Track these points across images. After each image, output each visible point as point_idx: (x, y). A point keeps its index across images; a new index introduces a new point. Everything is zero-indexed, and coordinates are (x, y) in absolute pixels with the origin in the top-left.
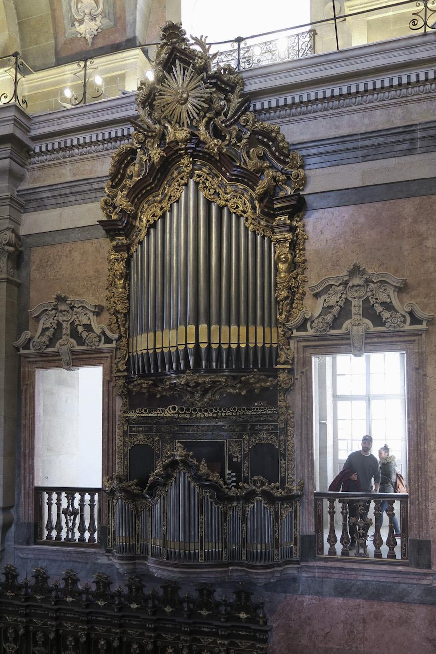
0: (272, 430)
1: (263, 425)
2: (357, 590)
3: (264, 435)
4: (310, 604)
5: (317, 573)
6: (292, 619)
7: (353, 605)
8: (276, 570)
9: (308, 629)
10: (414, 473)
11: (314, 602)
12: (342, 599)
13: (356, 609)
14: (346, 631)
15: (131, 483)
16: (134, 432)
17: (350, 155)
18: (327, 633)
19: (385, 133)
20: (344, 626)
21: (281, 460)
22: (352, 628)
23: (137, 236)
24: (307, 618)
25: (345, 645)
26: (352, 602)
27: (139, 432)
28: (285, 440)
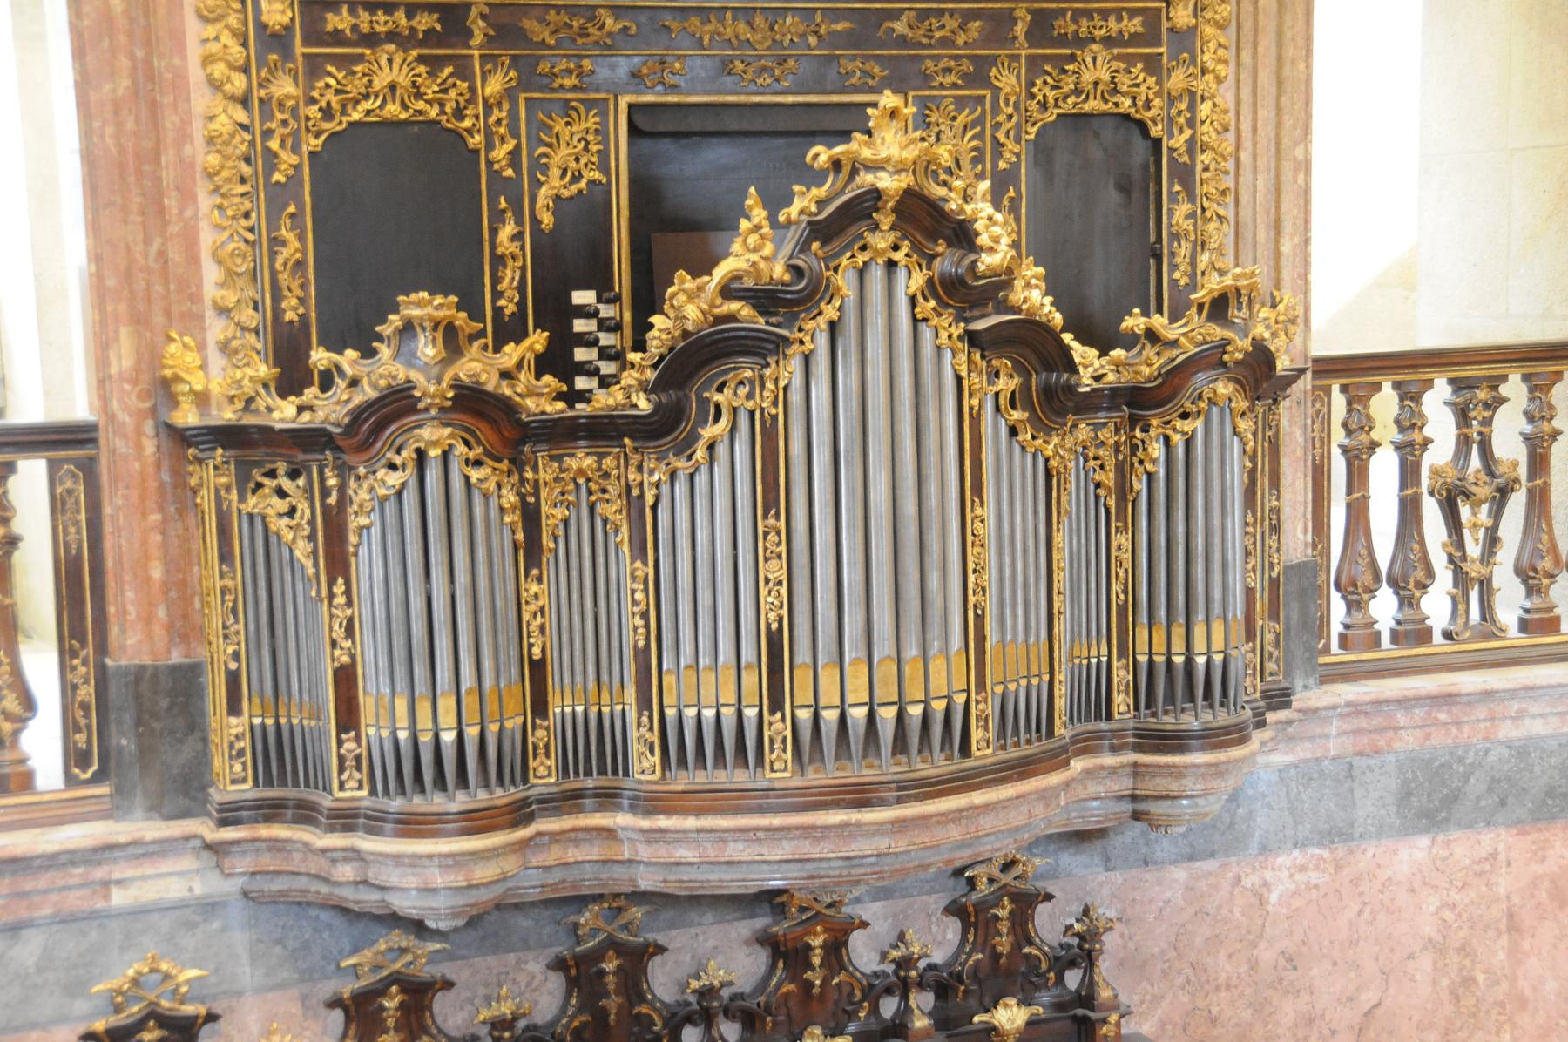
0: (1135, 40)
1: (1089, 14)
2: (1490, 789)
3: (1096, 67)
4: (1295, 894)
5: (1335, 741)
6: (1223, 978)
7: (1467, 862)
8: (540, 834)
9: (1288, 1011)
11: (1314, 877)
12: (1424, 841)
13: (1480, 874)
14: (1445, 982)
15: (511, 353)
16: (337, 38)
18: (1368, 1013)
20: (1435, 963)
21: (1173, 198)
22: (1467, 962)
24: (1282, 962)
27: (371, 40)
28: (1192, 94)
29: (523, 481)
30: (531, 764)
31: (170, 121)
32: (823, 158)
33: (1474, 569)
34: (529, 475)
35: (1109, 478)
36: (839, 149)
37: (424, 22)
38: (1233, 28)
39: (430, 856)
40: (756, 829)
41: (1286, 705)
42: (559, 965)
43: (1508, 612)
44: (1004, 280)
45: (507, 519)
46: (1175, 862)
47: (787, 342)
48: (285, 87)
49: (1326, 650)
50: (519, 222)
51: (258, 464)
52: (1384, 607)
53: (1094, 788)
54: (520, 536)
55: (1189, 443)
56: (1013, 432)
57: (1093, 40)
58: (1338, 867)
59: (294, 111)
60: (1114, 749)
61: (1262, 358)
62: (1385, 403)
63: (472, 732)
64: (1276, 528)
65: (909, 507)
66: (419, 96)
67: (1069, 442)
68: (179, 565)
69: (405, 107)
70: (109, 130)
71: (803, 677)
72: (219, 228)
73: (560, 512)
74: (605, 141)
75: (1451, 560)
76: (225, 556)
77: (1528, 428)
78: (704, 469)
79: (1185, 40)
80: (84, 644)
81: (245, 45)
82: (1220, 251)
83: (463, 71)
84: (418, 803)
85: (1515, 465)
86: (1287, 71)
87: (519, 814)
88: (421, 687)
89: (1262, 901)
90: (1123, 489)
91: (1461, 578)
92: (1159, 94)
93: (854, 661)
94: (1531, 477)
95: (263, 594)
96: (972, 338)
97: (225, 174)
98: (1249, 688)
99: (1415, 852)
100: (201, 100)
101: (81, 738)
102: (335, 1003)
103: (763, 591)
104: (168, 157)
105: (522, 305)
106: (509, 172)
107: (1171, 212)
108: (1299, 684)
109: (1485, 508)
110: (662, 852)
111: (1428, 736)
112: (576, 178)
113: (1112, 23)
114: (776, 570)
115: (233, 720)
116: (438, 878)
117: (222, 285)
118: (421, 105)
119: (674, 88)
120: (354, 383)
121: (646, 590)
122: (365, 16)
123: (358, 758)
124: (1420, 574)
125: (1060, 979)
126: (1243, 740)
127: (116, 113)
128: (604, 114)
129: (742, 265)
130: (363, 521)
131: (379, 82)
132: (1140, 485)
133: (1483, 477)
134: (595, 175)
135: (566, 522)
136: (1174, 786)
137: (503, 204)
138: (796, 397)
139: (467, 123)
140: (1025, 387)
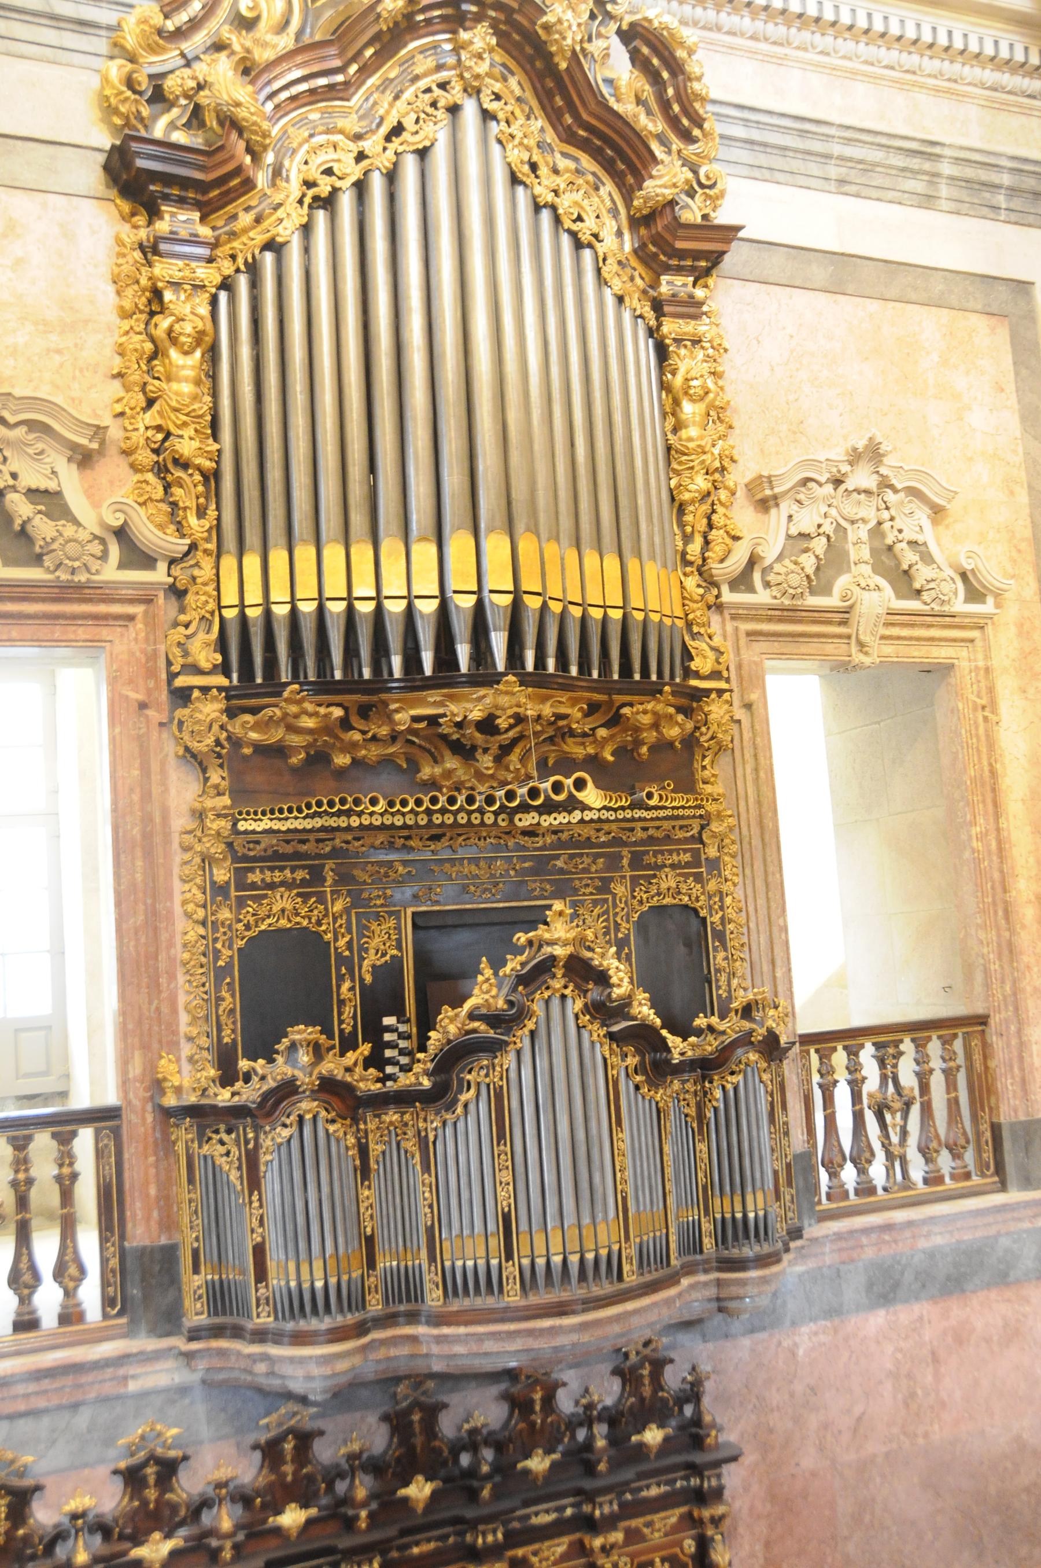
0: (688, 865)
1: (662, 852)
2: (916, 1279)
3: (668, 880)
5: (829, 1256)
6: (774, 1404)
9: (813, 1421)
10: (1000, 959)
11: (822, 1338)
12: (882, 1312)
14: (900, 1396)
15: (351, 1057)
16: (253, 886)
17: (814, 168)
18: (859, 1419)
19: (884, 141)
23: (258, 220)
25: (902, 1437)
26: (906, 1314)
27: (272, 886)
28: (721, 893)
29: (358, 1130)
30: (368, 1298)
31: (164, 936)
32: (523, 940)
33: (896, 1150)
34: (362, 1126)
35: (692, 1111)
36: (531, 934)
37: (300, 874)
38: (739, 857)
39: (311, 1357)
40: (500, 1333)
41: (800, 1237)
42: (386, 1418)
43: (917, 1174)
44: (627, 1001)
45: (350, 1153)
46: (744, 1335)
47: (507, 1043)
48: (225, 914)
49: (820, 1202)
50: (353, 980)
51: (209, 1126)
52: (849, 1174)
53: (695, 1295)
54: (358, 1162)
55: (736, 1089)
56: (637, 1088)
57: (665, 866)
58: (836, 1331)
59: (230, 927)
60: (706, 1271)
61: (772, 1038)
62: (840, 1058)
63: (332, 1281)
64: (787, 1134)
65: (581, 1135)
66: (297, 914)
67: (669, 1091)
68: (165, 1186)
69: (290, 921)
70: (132, 943)
71: (525, 1239)
72: (189, 993)
73: (380, 1148)
74: (400, 933)
75: (883, 1145)
76: (191, 1181)
77: (917, 1068)
78: (462, 1119)
79: (714, 865)
80: (113, 1235)
81: (204, 893)
82: (743, 977)
83: (321, 899)
84: (303, 1325)
85: (912, 1089)
86: (770, 878)
87: (361, 1329)
88: (303, 1255)
89: (794, 1354)
90: (701, 1117)
91: (890, 1156)
92: (703, 893)
93: (554, 1228)
94: (921, 1096)
95: (212, 1201)
96: (611, 1036)
97: (192, 963)
98: (780, 1229)
99: (877, 1320)
100: (181, 924)
101: (111, 1290)
102: (255, 1447)
103: (499, 1189)
104: (162, 956)
105: (355, 1026)
106: (347, 953)
107: (715, 958)
108: (806, 1223)
109: (899, 1115)
110: (446, 1349)
111: (880, 1250)
112: (384, 955)
113: (675, 857)
114: (506, 1176)
115: (196, 1277)
116: (316, 1371)
117: (190, 1024)
118: (298, 919)
119: (437, 903)
120: (263, 1078)
121: (431, 1191)
122: (268, 873)
123: (267, 1299)
124: (867, 1155)
125: (681, 1410)
126: (779, 1261)
127: (136, 934)
128: (398, 919)
129: (480, 1001)
130: (269, 1157)
131: (276, 909)
132: (710, 1114)
133: (896, 1097)
134: (395, 952)
135: (384, 1153)
136: (741, 1291)
137: (344, 971)
138: (513, 1075)
139: (323, 928)
140: (642, 1062)
